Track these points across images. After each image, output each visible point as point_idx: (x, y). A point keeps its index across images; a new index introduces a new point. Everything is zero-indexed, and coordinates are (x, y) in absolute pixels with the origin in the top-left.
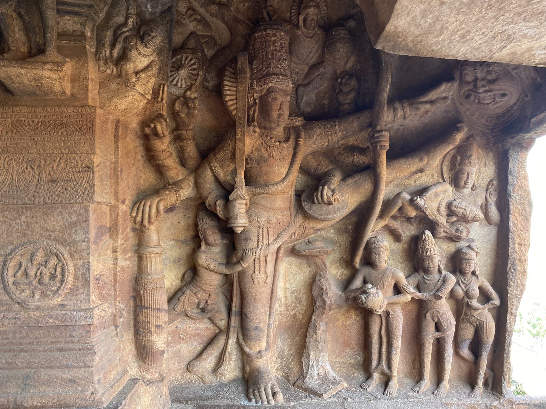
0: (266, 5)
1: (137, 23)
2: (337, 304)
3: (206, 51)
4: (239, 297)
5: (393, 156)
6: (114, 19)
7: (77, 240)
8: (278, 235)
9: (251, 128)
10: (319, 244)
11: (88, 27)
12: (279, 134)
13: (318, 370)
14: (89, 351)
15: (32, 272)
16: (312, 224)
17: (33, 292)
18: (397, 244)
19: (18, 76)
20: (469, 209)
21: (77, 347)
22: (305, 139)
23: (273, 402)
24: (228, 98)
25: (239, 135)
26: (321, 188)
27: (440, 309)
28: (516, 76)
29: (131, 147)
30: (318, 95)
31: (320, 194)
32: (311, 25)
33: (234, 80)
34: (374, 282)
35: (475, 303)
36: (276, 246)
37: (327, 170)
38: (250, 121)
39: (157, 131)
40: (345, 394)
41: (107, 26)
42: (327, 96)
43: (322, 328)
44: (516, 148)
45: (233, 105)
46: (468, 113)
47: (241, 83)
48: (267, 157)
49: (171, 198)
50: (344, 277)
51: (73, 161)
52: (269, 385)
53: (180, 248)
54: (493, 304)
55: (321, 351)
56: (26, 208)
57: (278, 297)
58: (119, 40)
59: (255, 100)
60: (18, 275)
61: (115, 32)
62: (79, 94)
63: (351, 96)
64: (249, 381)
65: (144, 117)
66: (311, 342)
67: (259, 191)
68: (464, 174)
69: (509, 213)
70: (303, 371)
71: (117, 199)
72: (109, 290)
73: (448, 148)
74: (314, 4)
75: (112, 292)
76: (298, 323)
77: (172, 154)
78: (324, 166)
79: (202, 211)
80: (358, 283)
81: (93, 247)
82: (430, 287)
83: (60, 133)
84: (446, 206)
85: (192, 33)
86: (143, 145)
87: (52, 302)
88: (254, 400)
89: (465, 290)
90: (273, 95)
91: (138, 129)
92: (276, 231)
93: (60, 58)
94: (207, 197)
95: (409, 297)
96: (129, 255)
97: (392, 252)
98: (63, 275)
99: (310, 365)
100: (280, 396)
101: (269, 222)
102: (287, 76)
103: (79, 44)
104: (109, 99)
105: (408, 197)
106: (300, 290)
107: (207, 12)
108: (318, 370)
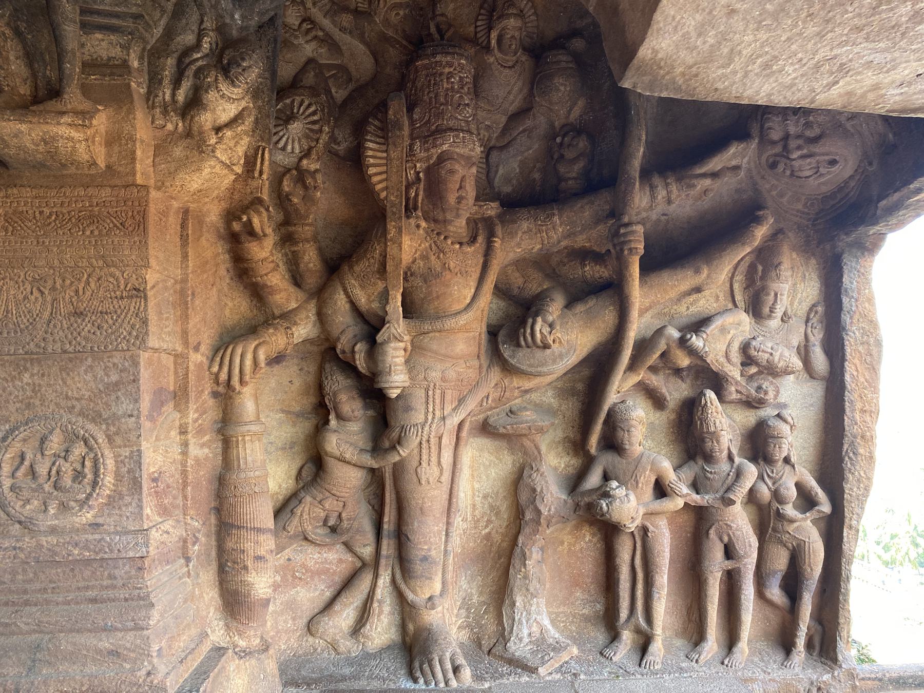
0: (434, 12)
1: (217, 46)
2: (559, 516)
3: (333, 91)
4: (394, 506)
5: (650, 266)
6: (178, 39)
7: (120, 413)
8: (459, 401)
9: (412, 221)
10: (528, 415)
11: (134, 51)
12: (460, 231)
13: (530, 628)
14: (142, 602)
15: (42, 470)
16: (516, 382)
17: (45, 503)
18: (658, 414)
19: (16, 136)
20: (778, 354)
21: (122, 596)
22: (503, 238)
23: (454, 683)
24: (372, 171)
25: (392, 233)
26: (530, 321)
27: (732, 521)
28: (852, 131)
29: (209, 254)
31: (529, 331)
32: (510, 46)
33: (382, 140)
35: (789, 510)
36: (456, 420)
37: (539, 289)
38: (410, 208)
39: (252, 228)
40: (575, 667)
42: (538, 165)
43: (535, 556)
44: (854, 250)
45: (380, 182)
46: (774, 193)
48: (439, 269)
49: (277, 340)
50: (571, 470)
51: (111, 280)
52: (448, 655)
53: (294, 424)
54: (819, 511)
55: (533, 596)
56: (32, 360)
57: (460, 505)
58: (187, 73)
59: (419, 173)
60: (19, 474)
61: (180, 61)
62: (120, 165)
63: (578, 167)
64: (414, 648)
65: (231, 203)
66: (517, 580)
67: (427, 327)
68: (768, 294)
69: (843, 359)
70: (504, 629)
71: (186, 343)
72: (175, 498)
73: (741, 253)
74: (515, 12)
75: (180, 501)
76: (494, 549)
77: (278, 266)
78: (536, 284)
79: (329, 361)
80: (594, 480)
81: (146, 424)
82: (715, 484)
83: (88, 233)
84: (740, 348)
85: (310, 61)
86: (229, 252)
87: (77, 520)
88: (422, 681)
89: (773, 488)
90: (448, 165)
91: (221, 225)
92: (456, 394)
93: (86, 105)
94: (338, 339)
95: (680, 503)
96: (207, 438)
97: (651, 427)
98: (96, 473)
100: (467, 673)
101: (443, 379)
102: (472, 133)
103: (119, 81)
104: (172, 174)
105: (676, 334)
106: (498, 493)
107: (335, 26)
108: (530, 628)
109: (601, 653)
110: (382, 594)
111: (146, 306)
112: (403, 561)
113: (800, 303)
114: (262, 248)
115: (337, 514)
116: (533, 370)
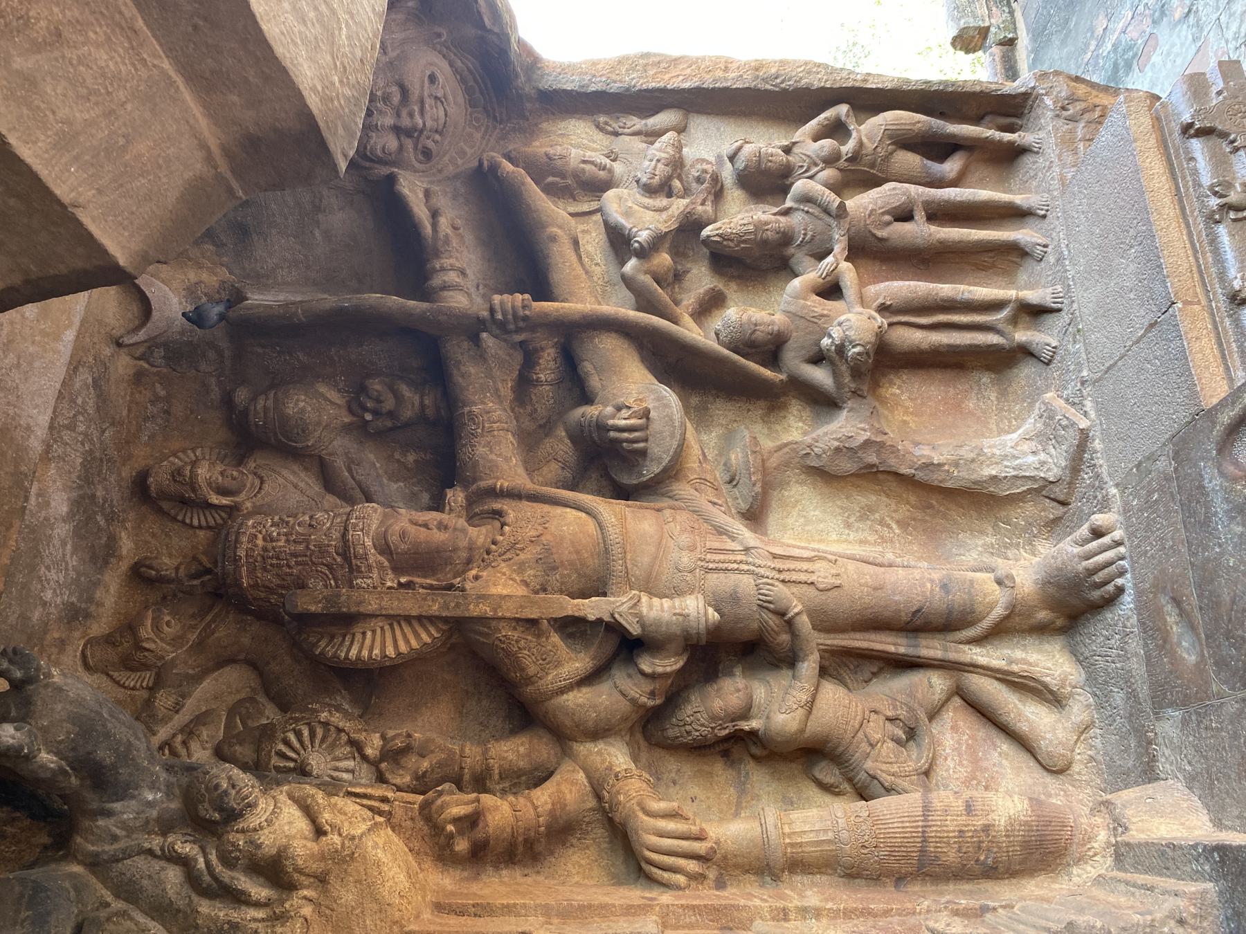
2: (871, 417)
4: (873, 636)
5: (543, 290)
6: (171, 893)
8: (720, 533)
9: (468, 585)
10: (736, 457)
13: (1025, 454)
24: (390, 651)
25: (485, 609)
26: (612, 434)
27: (865, 208)
28: (398, 51)
29: (503, 889)
30: (393, 477)
31: (626, 435)
32: (234, 479)
35: (848, 147)
37: (567, 441)
39: (466, 817)
41: (185, 913)
42: (397, 456)
43: (926, 453)
44: (535, 76)
45: (407, 641)
46: (460, 162)
47: (360, 603)
48: (539, 549)
50: (807, 413)
52: (1077, 550)
53: (757, 797)
54: (847, 115)
55: (981, 452)
58: (227, 880)
59: (400, 585)
64: (1073, 607)
65: (426, 854)
66: (960, 477)
67: (618, 567)
68: (583, 170)
69: (663, 91)
70: (1029, 491)
73: (533, 191)
76: (919, 515)
78: (560, 445)
80: (820, 376)
82: (819, 229)
86: (497, 868)
88: (1119, 581)
90: (393, 539)
91: (458, 873)
94: (633, 701)
95: (845, 266)
101: (692, 548)
104: (382, 907)
105: (631, 265)
106: (842, 508)
107: (171, 719)
108: (1025, 454)
109: (1048, 364)
110: (998, 658)
112: (949, 622)
113: (595, 142)
114: (497, 808)
115: (888, 724)
116: (678, 432)
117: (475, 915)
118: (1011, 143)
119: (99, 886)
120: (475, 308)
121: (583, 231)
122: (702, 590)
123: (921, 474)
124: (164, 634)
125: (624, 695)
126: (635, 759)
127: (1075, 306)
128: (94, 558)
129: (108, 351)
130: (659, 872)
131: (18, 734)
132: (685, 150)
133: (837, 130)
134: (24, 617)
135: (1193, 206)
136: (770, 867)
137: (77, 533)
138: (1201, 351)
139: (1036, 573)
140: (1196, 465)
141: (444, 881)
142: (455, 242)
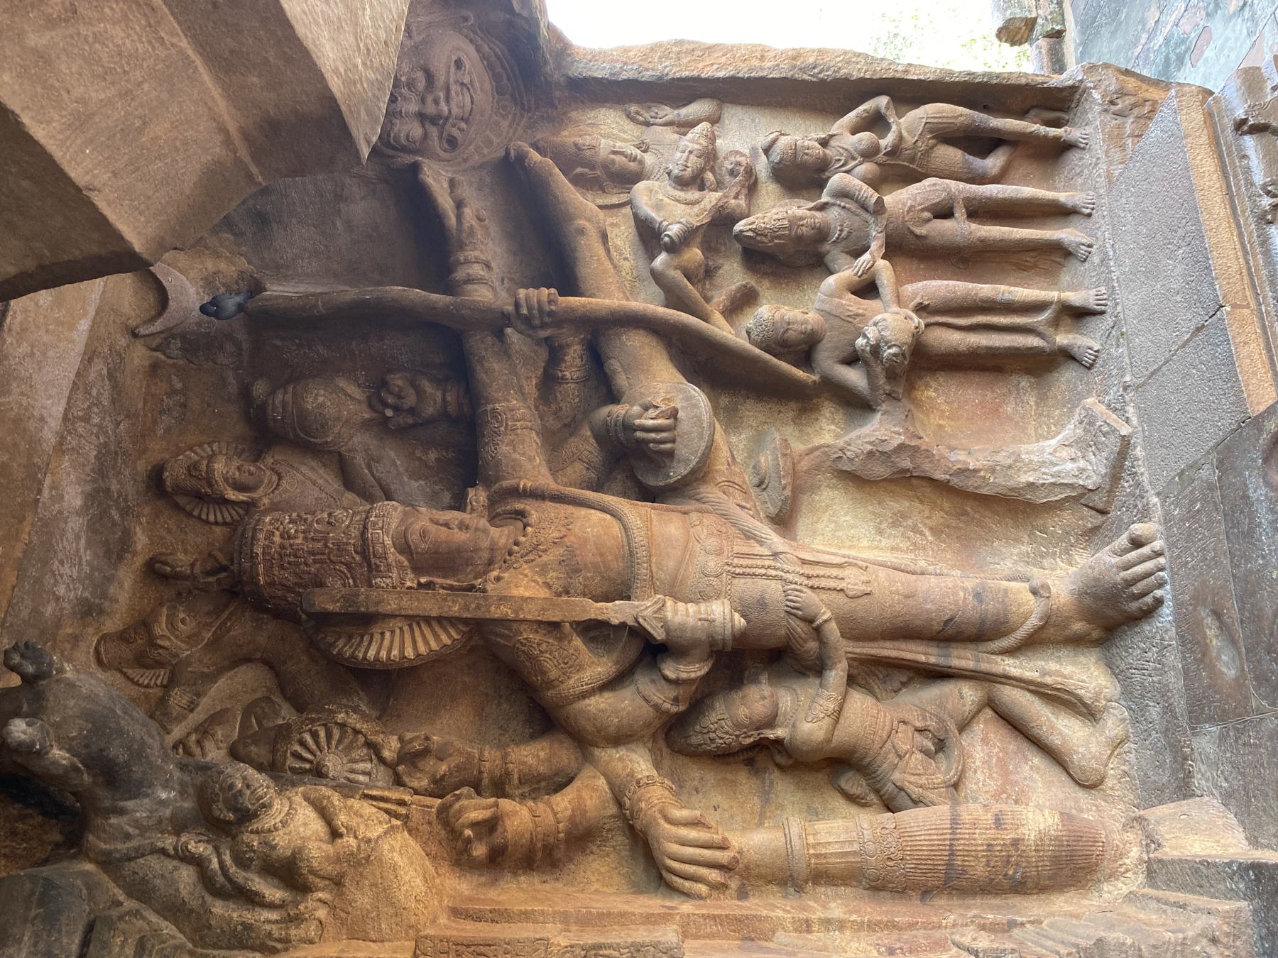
0: (186, 578)
2: (905, 421)
3: (281, 722)
4: (903, 645)
6: (184, 893)
8: (748, 538)
9: (489, 587)
10: (765, 460)
13: (1064, 460)
24: (409, 653)
25: (505, 611)
26: (638, 434)
27: (904, 205)
28: (424, 35)
29: (522, 895)
30: (414, 476)
31: (653, 435)
32: (251, 474)
33: (366, 638)
34: (851, 337)
35: (887, 141)
41: (198, 913)
42: (418, 453)
44: (564, 63)
45: (426, 643)
46: (486, 151)
47: (378, 603)
50: (839, 416)
52: (1115, 560)
53: (782, 807)
54: (887, 108)
59: (420, 585)
61: (219, 893)
63: (427, 387)
64: (1110, 619)
65: (443, 858)
66: (996, 483)
68: (613, 161)
69: (697, 80)
70: (1068, 499)
78: (585, 445)
80: (854, 377)
82: (856, 225)
84: (682, 190)
86: (515, 874)
88: (1158, 593)
90: (414, 538)
91: (475, 879)
94: (656, 707)
95: (882, 264)
99: (1052, 480)
101: (719, 553)
104: (398, 912)
105: (661, 260)
106: (874, 513)
107: (185, 718)
108: (1064, 460)
109: (1089, 368)
110: (1031, 670)
111: (610, 947)
112: (981, 632)
113: (625, 132)
115: (916, 735)
117: (492, 921)
118: (1057, 139)
119: (111, 885)
120: (499, 303)
121: (612, 225)
122: (728, 595)
123: (956, 480)
124: (179, 631)
125: (647, 701)
126: (657, 765)
127: (1119, 308)
128: (108, 553)
129: (123, 342)
130: (680, 881)
131: (30, 730)
132: (719, 142)
133: (876, 122)
134: (36, 612)
135: (1244, 205)
136: (791, 878)
137: (92, 528)
138: (1249, 357)
139: (1072, 583)
140: (1241, 474)
141: (461, 886)
142: (480, 234)
